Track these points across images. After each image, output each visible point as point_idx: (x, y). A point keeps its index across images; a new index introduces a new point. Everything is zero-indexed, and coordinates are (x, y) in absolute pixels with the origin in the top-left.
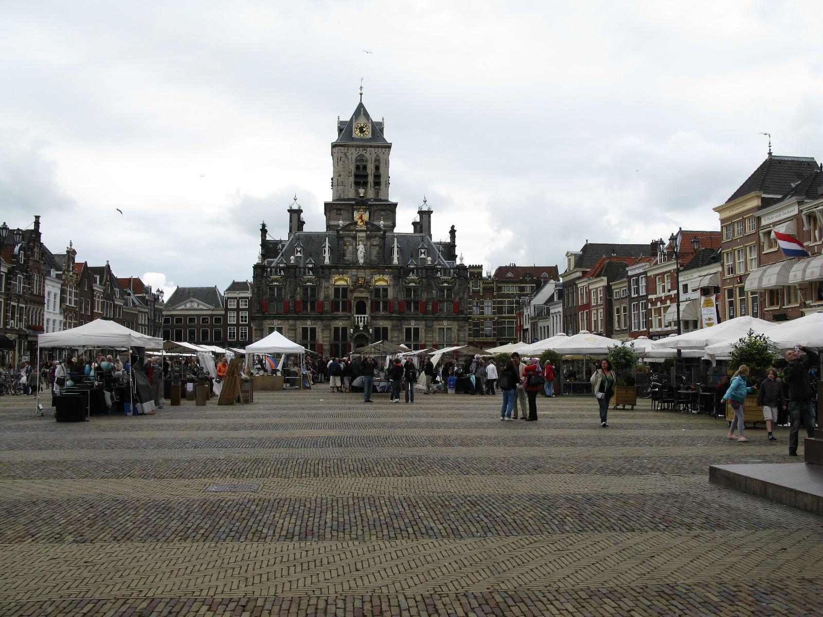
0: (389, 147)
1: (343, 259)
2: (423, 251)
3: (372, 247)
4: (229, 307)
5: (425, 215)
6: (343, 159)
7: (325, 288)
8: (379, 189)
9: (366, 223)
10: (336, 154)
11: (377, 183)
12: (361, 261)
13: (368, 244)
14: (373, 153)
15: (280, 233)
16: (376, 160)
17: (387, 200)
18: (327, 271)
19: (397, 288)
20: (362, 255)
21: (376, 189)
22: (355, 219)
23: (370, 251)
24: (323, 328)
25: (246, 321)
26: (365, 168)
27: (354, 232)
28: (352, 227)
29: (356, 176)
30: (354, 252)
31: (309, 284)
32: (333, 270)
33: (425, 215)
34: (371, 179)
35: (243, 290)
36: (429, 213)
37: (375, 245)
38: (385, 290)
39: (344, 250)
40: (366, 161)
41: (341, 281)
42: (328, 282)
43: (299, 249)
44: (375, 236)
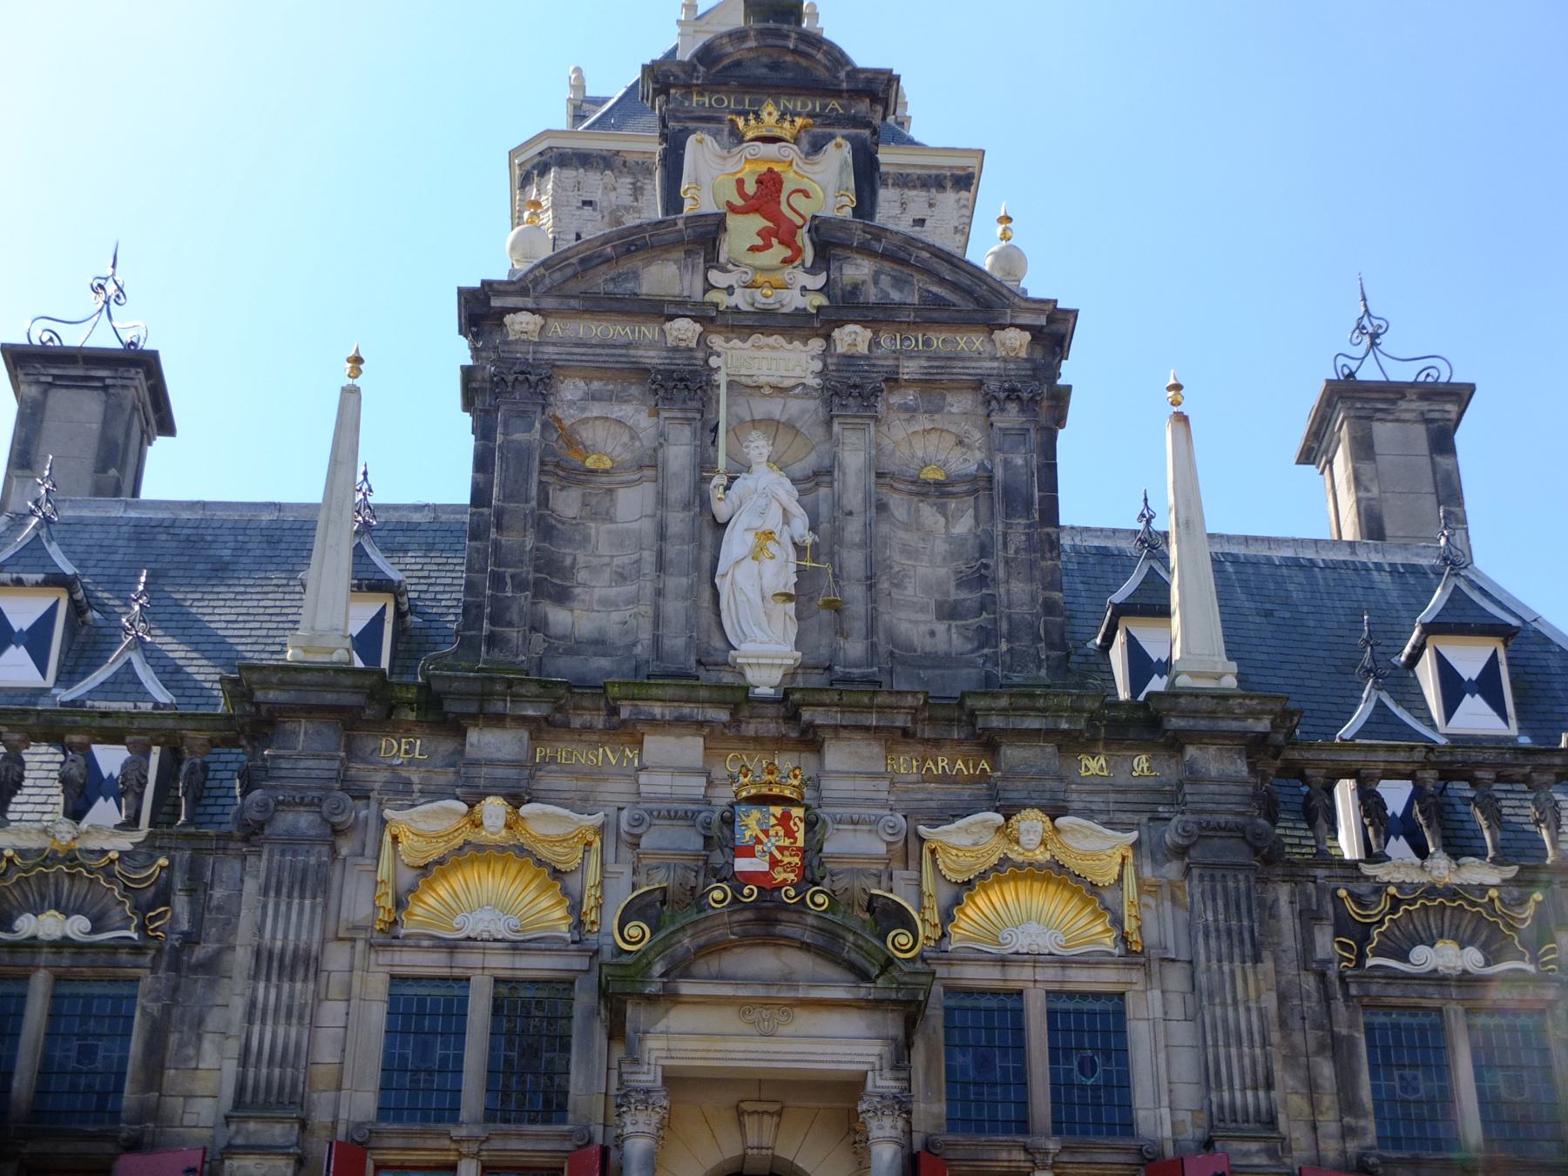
1: (538, 625)
2: (1470, 658)
3: (899, 505)
5: (1395, 421)
7: (266, 962)
12: (765, 646)
13: (853, 459)
18: (305, 751)
19: (1256, 990)
20: (780, 572)
23: (869, 541)
27: (684, 330)
31: (47, 925)
32: (400, 751)
33: (1395, 421)
37: (940, 491)
38: (1092, 1031)
39: (546, 529)
41: (479, 879)
42: (313, 884)
43: (23, 611)
44: (933, 386)
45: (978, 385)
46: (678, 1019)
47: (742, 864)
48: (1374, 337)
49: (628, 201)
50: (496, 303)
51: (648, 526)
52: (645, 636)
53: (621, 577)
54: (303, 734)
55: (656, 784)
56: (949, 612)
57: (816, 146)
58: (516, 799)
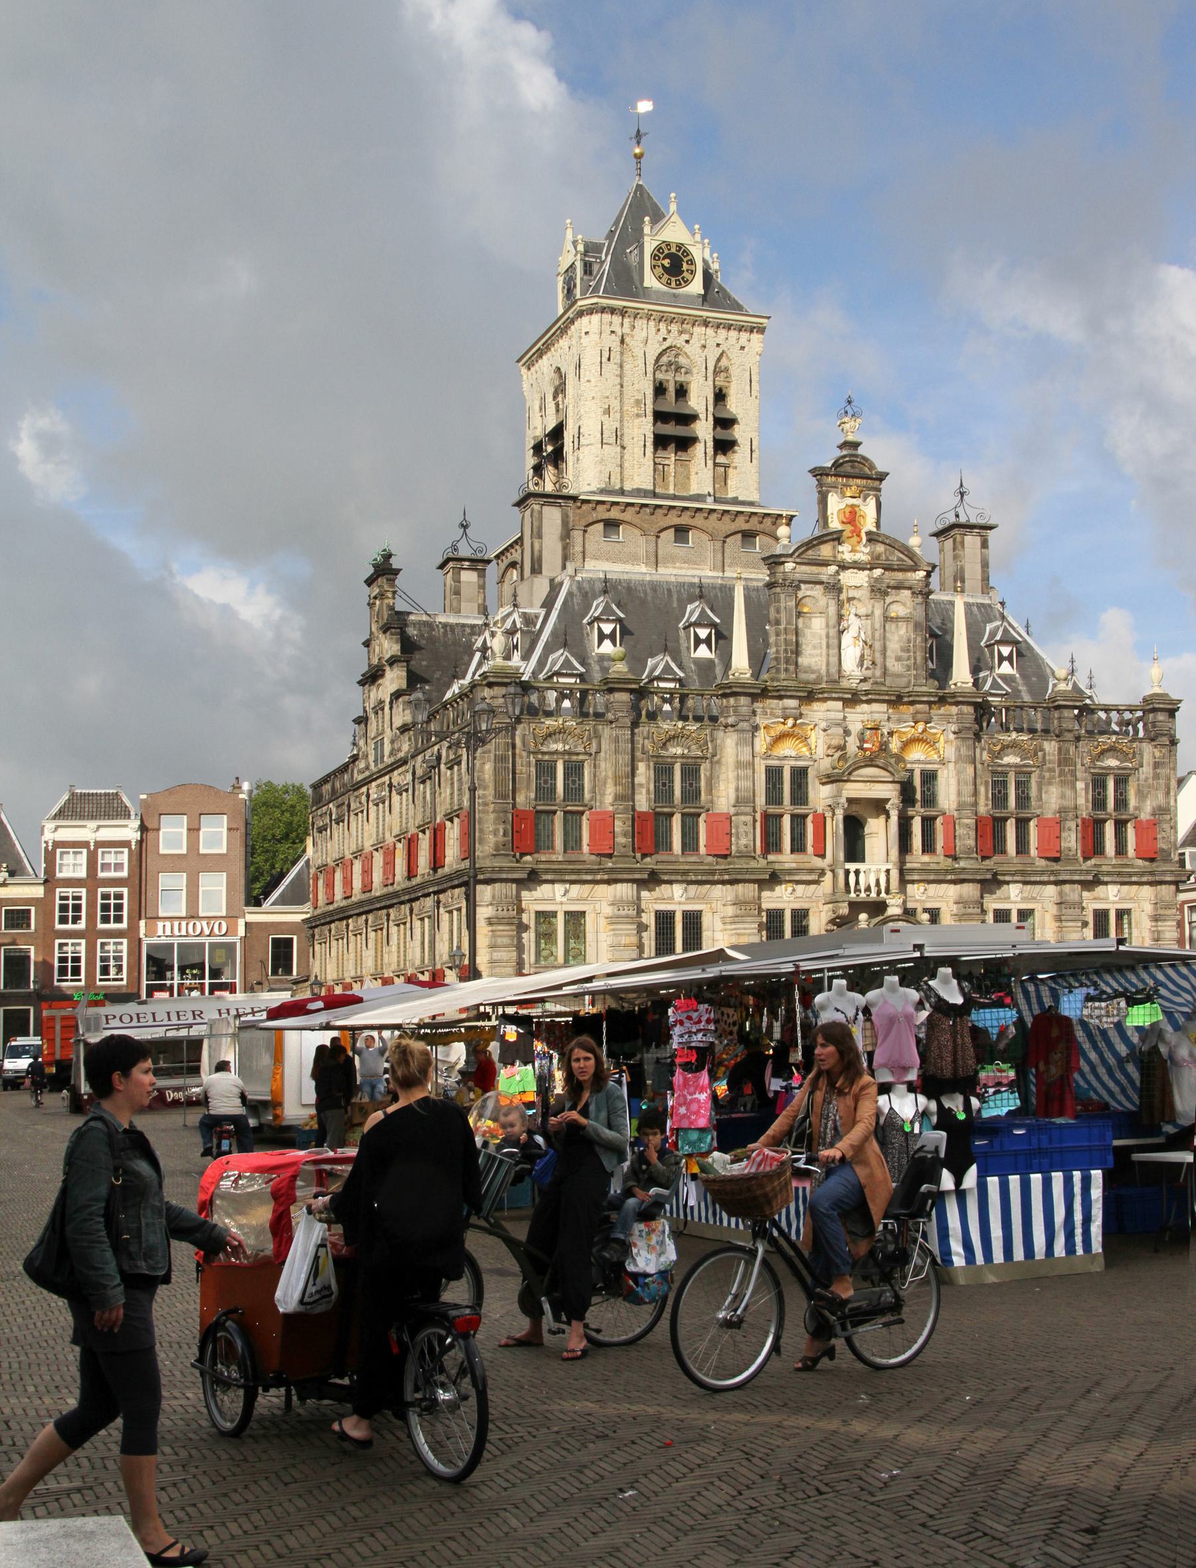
2: (1006, 651)
4: (59, 875)
6: (616, 357)
8: (726, 467)
9: (872, 538)
10: (594, 337)
11: (724, 446)
13: (878, 612)
14: (711, 343)
21: (715, 465)
22: (835, 524)
24: (730, 911)
25: (118, 919)
27: (832, 569)
28: (826, 551)
29: (659, 416)
30: (834, 642)
34: (704, 430)
35: (109, 816)
37: (896, 619)
43: (607, 628)
44: (898, 587)
45: (910, 588)
46: (849, 785)
47: (866, 746)
48: (962, 494)
49: (626, 329)
50: (783, 559)
51: (824, 633)
52: (824, 668)
53: (815, 647)
54: (743, 700)
55: (832, 715)
56: (898, 659)
57: (865, 500)
58: (796, 719)
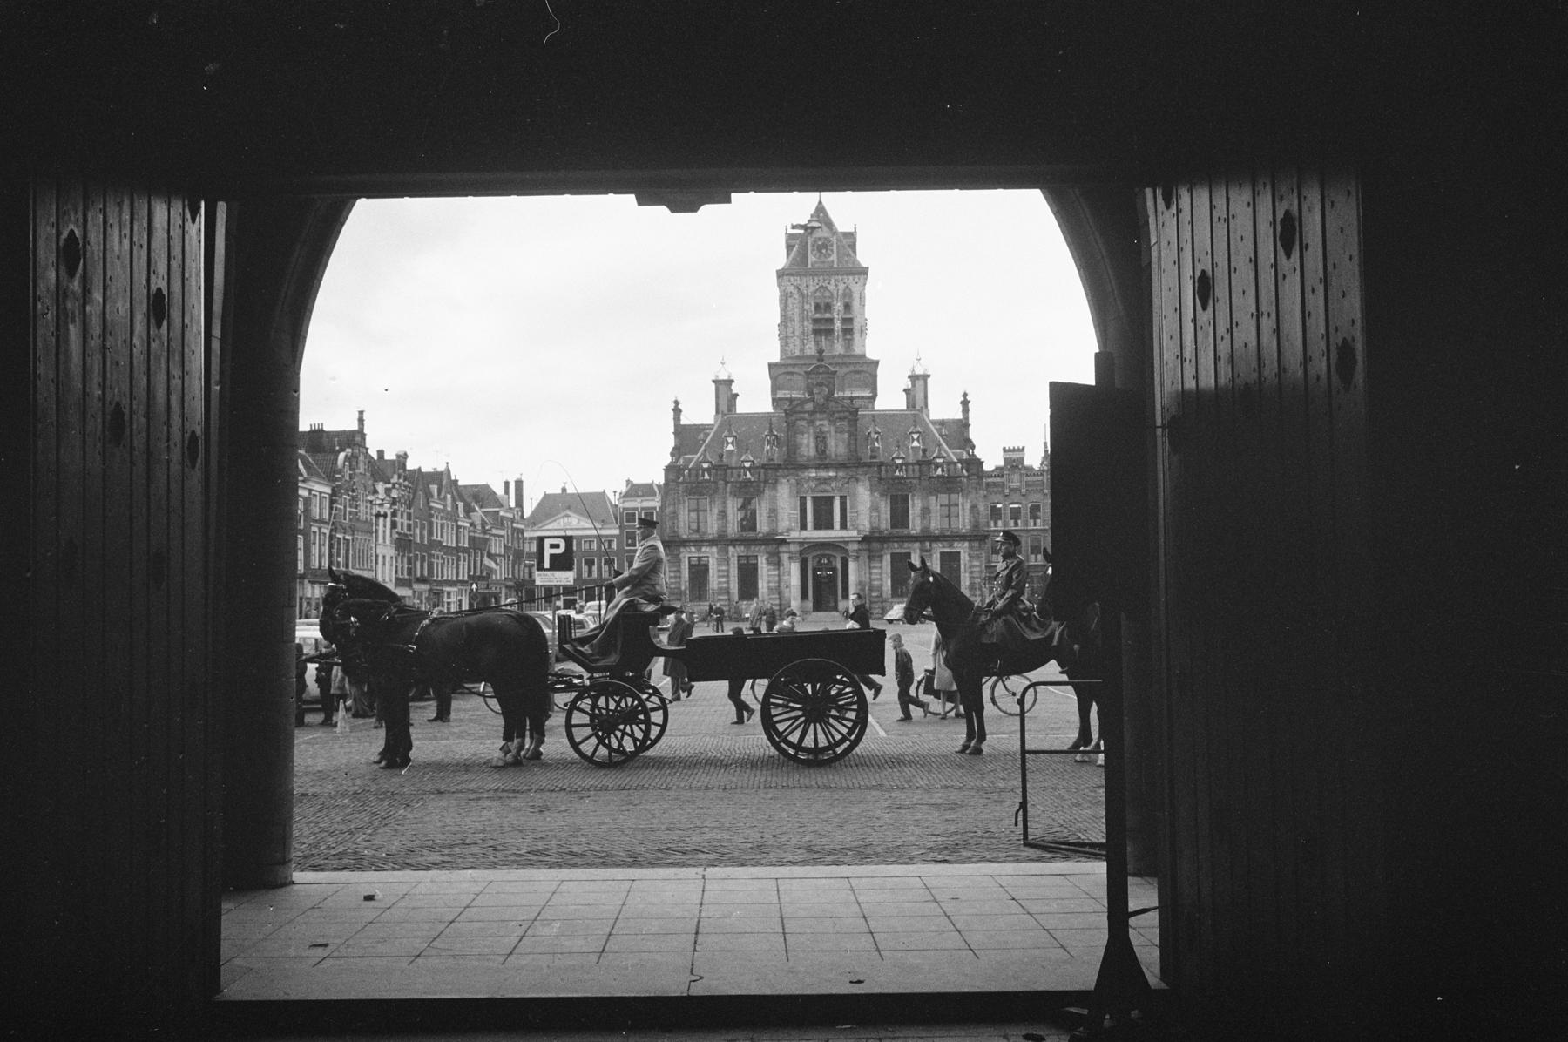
0: (864, 272)
5: (919, 381)
11: (848, 331)
15: (702, 412)
16: (845, 295)
17: (864, 356)
26: (828, 307)
33: (919, 381)
36: (925, 377)
40: (832, 296)
